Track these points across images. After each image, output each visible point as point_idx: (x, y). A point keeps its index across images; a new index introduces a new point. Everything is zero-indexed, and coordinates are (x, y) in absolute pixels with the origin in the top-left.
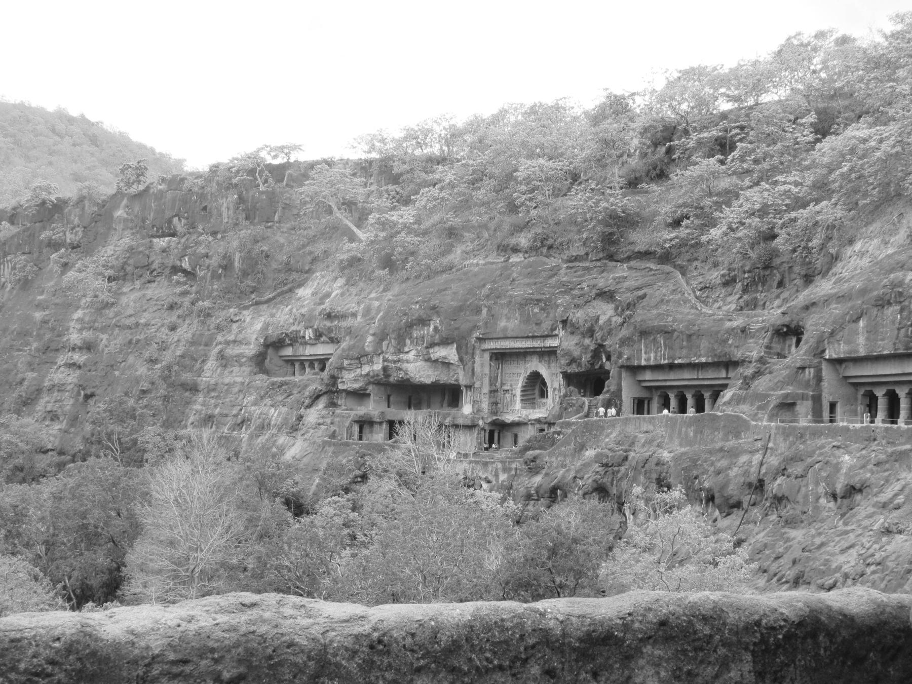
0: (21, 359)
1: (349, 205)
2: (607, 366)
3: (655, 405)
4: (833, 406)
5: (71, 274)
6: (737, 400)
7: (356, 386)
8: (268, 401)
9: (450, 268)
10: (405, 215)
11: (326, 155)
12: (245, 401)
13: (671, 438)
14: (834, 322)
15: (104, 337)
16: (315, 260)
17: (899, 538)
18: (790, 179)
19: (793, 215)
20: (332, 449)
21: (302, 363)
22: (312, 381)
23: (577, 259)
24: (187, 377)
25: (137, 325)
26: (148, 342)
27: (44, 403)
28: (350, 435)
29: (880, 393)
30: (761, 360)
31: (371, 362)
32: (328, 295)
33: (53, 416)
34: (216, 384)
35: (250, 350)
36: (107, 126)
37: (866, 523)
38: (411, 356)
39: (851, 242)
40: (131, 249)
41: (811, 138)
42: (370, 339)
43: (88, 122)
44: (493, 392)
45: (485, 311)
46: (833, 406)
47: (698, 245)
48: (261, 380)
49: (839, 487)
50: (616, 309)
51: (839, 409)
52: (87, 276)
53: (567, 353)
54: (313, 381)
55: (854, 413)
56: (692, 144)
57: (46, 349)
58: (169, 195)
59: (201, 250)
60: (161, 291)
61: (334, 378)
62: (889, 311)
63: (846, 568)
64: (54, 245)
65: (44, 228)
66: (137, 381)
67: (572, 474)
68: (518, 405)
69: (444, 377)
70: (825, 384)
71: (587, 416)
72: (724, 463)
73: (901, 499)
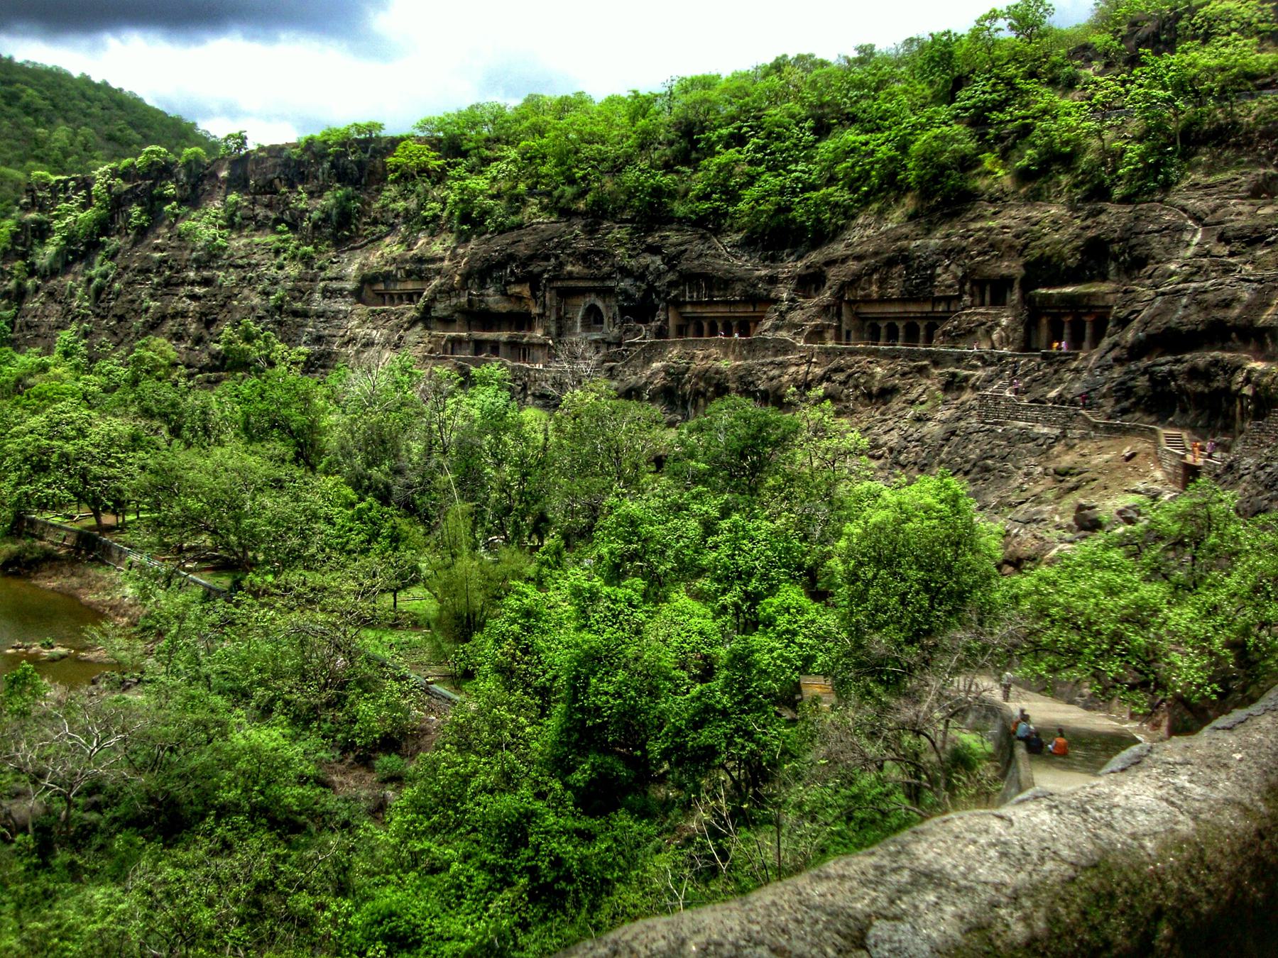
0: (144, 291)
1: (424, 171)
2: (656, 301)
3: (691, 329)
4: (848, 333)
5: (183, 225)
6: (776, 328)
7: (445, 314)
8: (371, 325)
9: (520, 226)
10: (478, 183)
11: (404, 133)
12: (350, 325)
13: (726, 355)
14: (853, 274)
15: (222, 274)
16: (397, 216)
17: (930, 424)
18: (799, 168)
19: (807, 195)
20: (432, 362)
21: (391, 296)
22: (411, 311)
23: (627, 221)
24: (298, 305)
25: (249, 264)
26: (260, 278)
27: (170, 325)
28: (445, 352)
29: (883, 325)
30: (792, 300)
31: (458, 296)
32: (415, 244)
33: (178, 337)
34: (324, 312)
35: (350, 285)
36: (126, 90)
37: (899, 414)
38: (491, 291)
39: (854, 217)
40: (237, 202)
41: (812, 138)
42: (457, 278)
43: (111, 88)
44: (559, 319)
45: (553, 260)
46: (848, 333)
47: (726, 214)
48: (361, 309)
49: (875, 389)
50: (663, 260)
51: (853, 335)
52: (203, 225)
53: (624, 292)
54: (409, 310)
55: (862, 339)
56: (714, 138)
57: (168, 283)
58: (270, 162)
59: (302, 205)
60: (271, 238)
61: (428, 308)
62: (896, 270)
63: (890, 444)
64: (168, 200)
65: (153, 185)
66: (253, 309)
67: (644, 380)
68: (579, 330)
69: (516, 308)
70: (844, 318)
71: (644, 338)
72: (776, 372)
73: (924, 398)
